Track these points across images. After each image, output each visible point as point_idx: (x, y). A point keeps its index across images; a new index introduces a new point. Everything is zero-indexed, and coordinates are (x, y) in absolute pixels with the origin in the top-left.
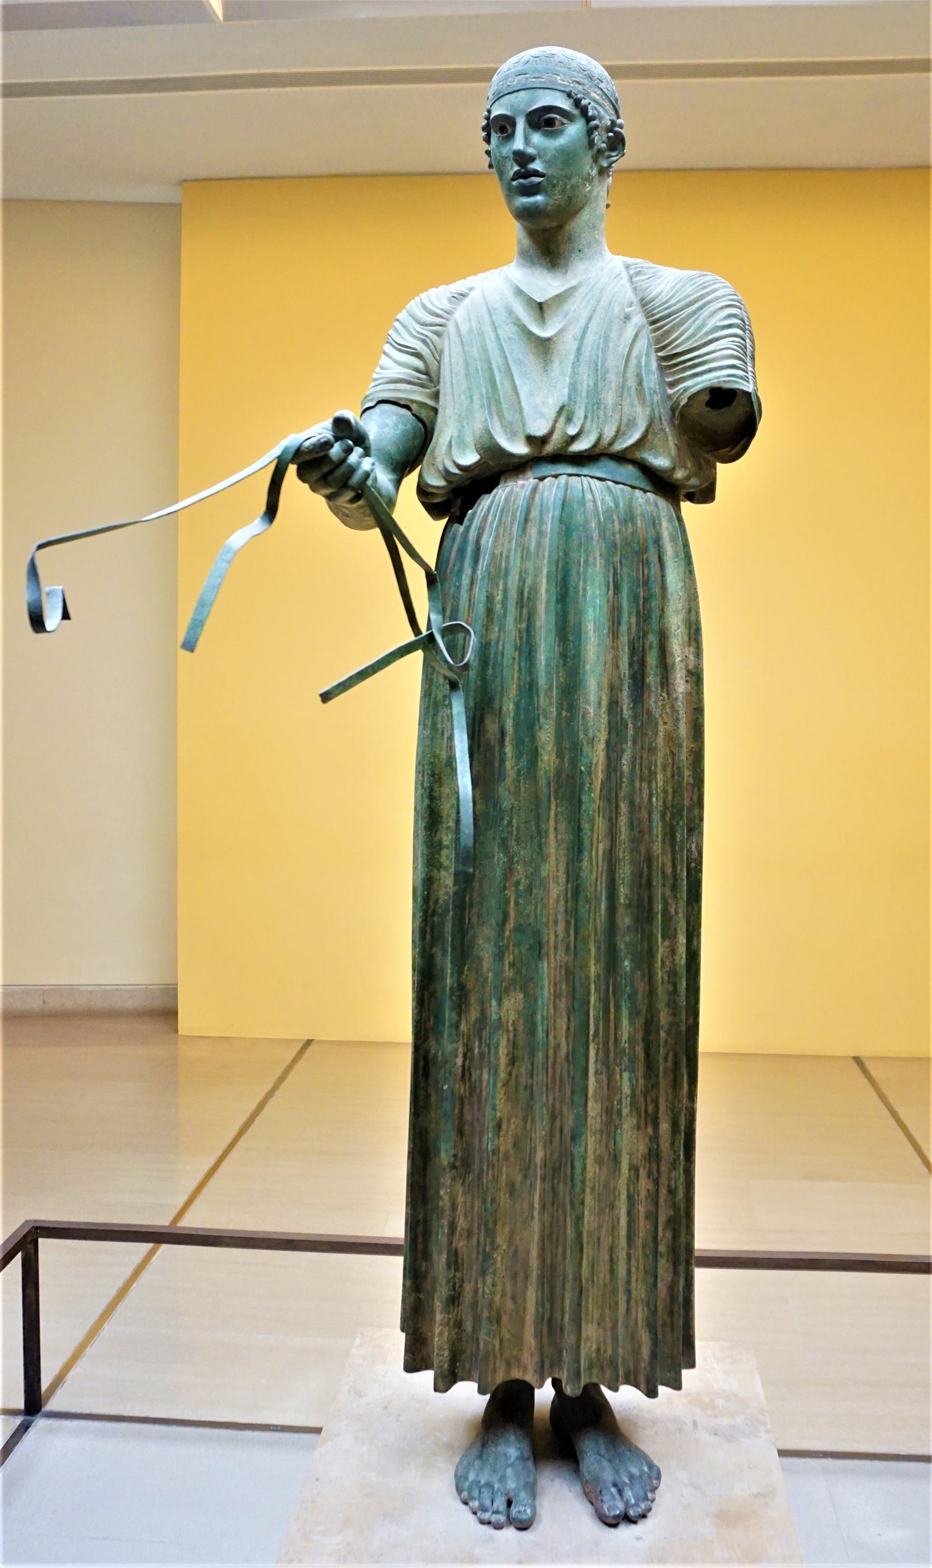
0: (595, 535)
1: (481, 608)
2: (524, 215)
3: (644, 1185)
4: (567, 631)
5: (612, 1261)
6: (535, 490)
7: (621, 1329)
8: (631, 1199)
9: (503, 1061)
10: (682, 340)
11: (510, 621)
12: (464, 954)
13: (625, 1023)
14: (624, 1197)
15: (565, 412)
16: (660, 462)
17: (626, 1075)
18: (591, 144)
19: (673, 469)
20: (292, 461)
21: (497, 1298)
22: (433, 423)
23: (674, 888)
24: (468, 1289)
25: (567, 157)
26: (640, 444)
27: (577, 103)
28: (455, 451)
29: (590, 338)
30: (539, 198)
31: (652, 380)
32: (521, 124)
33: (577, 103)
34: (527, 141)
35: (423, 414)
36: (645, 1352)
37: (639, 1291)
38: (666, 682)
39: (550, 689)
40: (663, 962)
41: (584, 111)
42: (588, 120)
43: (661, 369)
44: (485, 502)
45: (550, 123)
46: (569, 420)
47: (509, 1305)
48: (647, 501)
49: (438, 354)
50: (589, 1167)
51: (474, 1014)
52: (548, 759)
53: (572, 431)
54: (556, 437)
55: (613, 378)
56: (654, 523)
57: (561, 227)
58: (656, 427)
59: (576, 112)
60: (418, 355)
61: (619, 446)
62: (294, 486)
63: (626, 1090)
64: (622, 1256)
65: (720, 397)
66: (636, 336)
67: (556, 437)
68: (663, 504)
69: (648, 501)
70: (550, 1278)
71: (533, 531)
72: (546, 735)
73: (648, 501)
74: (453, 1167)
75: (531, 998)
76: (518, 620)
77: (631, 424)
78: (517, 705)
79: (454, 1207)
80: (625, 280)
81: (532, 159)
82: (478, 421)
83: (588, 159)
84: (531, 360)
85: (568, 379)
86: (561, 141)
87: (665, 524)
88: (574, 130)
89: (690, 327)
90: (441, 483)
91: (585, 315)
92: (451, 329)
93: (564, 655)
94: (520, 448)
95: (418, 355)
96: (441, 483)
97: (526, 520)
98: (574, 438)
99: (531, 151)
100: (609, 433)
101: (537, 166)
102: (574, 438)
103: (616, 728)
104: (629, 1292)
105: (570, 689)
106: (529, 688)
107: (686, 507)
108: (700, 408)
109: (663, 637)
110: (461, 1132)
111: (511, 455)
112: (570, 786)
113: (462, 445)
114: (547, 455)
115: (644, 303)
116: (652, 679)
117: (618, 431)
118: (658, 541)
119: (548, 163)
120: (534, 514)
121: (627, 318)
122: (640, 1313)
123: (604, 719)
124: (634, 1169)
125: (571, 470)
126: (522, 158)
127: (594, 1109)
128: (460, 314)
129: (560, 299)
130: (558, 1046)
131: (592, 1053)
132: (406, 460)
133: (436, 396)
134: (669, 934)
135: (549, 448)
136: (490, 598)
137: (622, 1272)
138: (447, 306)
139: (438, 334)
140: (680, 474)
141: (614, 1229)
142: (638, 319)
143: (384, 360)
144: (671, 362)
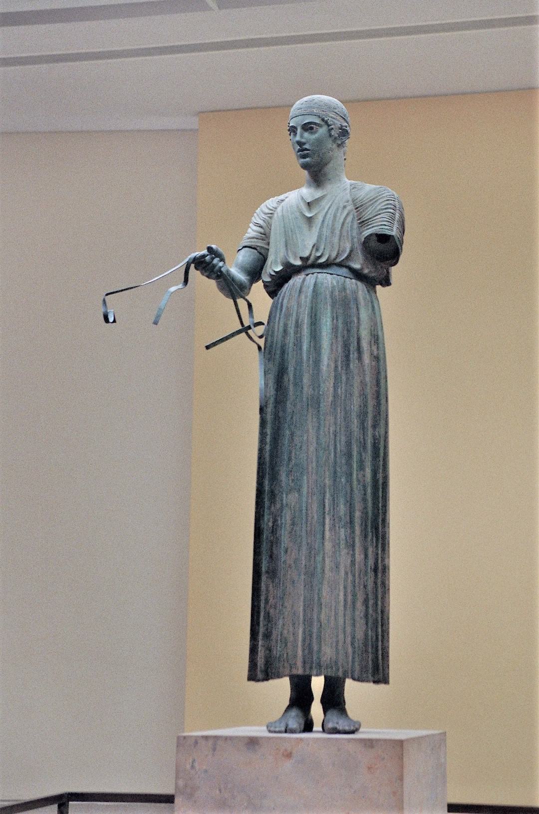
0: (328, 297)
1: (281, 329)
2: (305, 166)
3: (350, 577)
4: (315, 336)
5: (336, 614)
6: (304, 280)
7: (341, 644)
8: (345, 588)
9: (289, 522)
10: (367, 215)
11: (292, 335)
12: (274, 477)
13: (342, 506)
14: (342, 587)
15: (316, 247)
16: (357, 266)
17: (342, 530)
18: (330, 136)
19: (362, 269)
20: (193, 262)
21: (285, 632)
22: (267, 255)
23: (365, 447)
24: (274, 632)
25: (319, 142)
26: (348, 258)
27: (323, 120)
28: (274, 266)
29: (328, 216)
30: (308, 159)
31: (355, 234)
32: (299, 130)
33: (323, 120)
34: (302, 136)
35: (263, 251)
36: (350, 658)
37: (349, 629)
38: (360, 358)
39: (308, 360)
40: (358, 481)
41: (326, 122)
42: (329, 126)
43: (359, 228)
44: (286, 285)
45: (312, 128)
46: (317, 250)
47: (292, 638)
48: (352, 284)
49: (269, 225)
50: (326, 572)
51: (278, 506)
52: (307, 390)
53: (318, 254)
54: (312, 258)
55: (337, 232)
56: (355, 293)
57: (320, 171)
58: (354, 252)
59: (323, 123)
60: (261, 227)
61: (338, 260)
62: (194, 273)
63: (343, 536)
64: (341, 613)
65: (383, 238)
66: (348, 214)
67: (312, 258)
68: (359, 283)
69: (352, 283)
70: (308, 622)
71: (303, 297)
72: (306, 380)
73: (352, 283)
74: (267, 572)
75: (300, 495)
76: (296, 333)
77: (344, 251)
78: (295, 369)
79: (267, 590)
80: (348, 191)
81: (304, 144)
82: (282, 253)
83: (330, 141)
84: (305, 227)
85: (317, 234)
86: (316, 135)
87: (360, 292)
88: (323, 131)
89: (370, 209)
90: (269, 279)
91: (327, 207)
92: (275, 215)
93: (315, 347)
94: (298, 263)
95: (261, 227)
96: (269, 279)
97: (300, 292)
98: (319, 257)
99: (303, 140)
100: (334, 255)
101: (306, 146)
102: (319, 257)
103: (337, 378)
104: (345, 632)
105: (317, 362)
106: (299, 363)
107: (378, 287)
108: (374, 244)
109: (359, 340)
110: (271, 557)
111: (295, 266)
112: (315, 402)
113: (276, 262)
114: (309, 265)
115: (353, 201)
116: (354, 356)
117: (338, 254)
118: (356, 300)
119: (312, 145)
120: (304, 289)
121: (345, 207)
122: (349, 639)
123: (333, 374)
124: (346, 573)
125: (318, 271)
126: (300, 143)
127: (328, 545)
128: (279, 209)
129: (317, 201)
130: (313, 517)
131: (327, 521)
132: (255, 273)
133: (268, 244)
134: (361, 467)
135: (310, 262)
136: (286, 325)
137: (341, 620)
138: (275, 205)
139: (270, 218)
140: (366, 271)
141: (337, 603)
142: (350, 207)
143: (249, 230)
144: (363, 223)
